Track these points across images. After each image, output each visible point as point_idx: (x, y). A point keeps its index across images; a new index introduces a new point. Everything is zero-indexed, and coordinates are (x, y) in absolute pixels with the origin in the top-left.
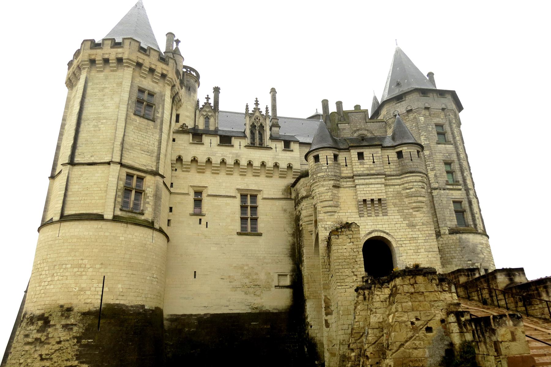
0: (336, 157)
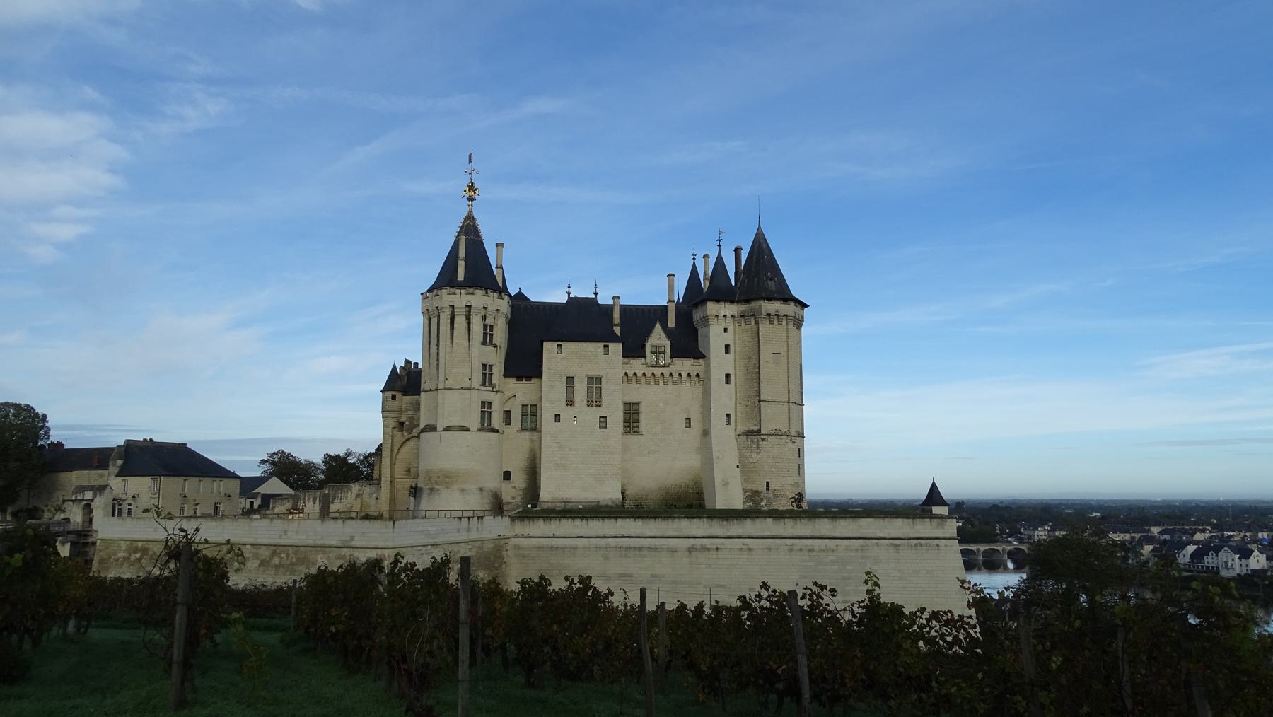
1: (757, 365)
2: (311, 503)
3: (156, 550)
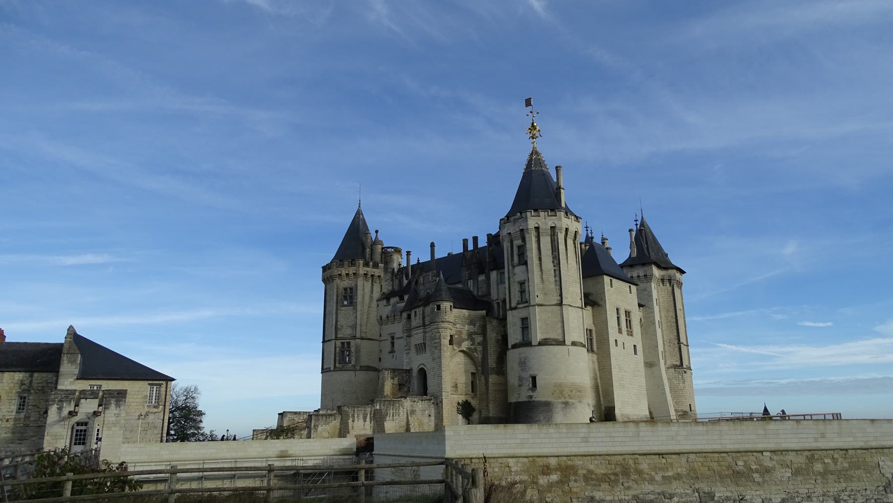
0: (409, 317)
1: (674, 316)
2: (361, 421)
3: (592, 467)
